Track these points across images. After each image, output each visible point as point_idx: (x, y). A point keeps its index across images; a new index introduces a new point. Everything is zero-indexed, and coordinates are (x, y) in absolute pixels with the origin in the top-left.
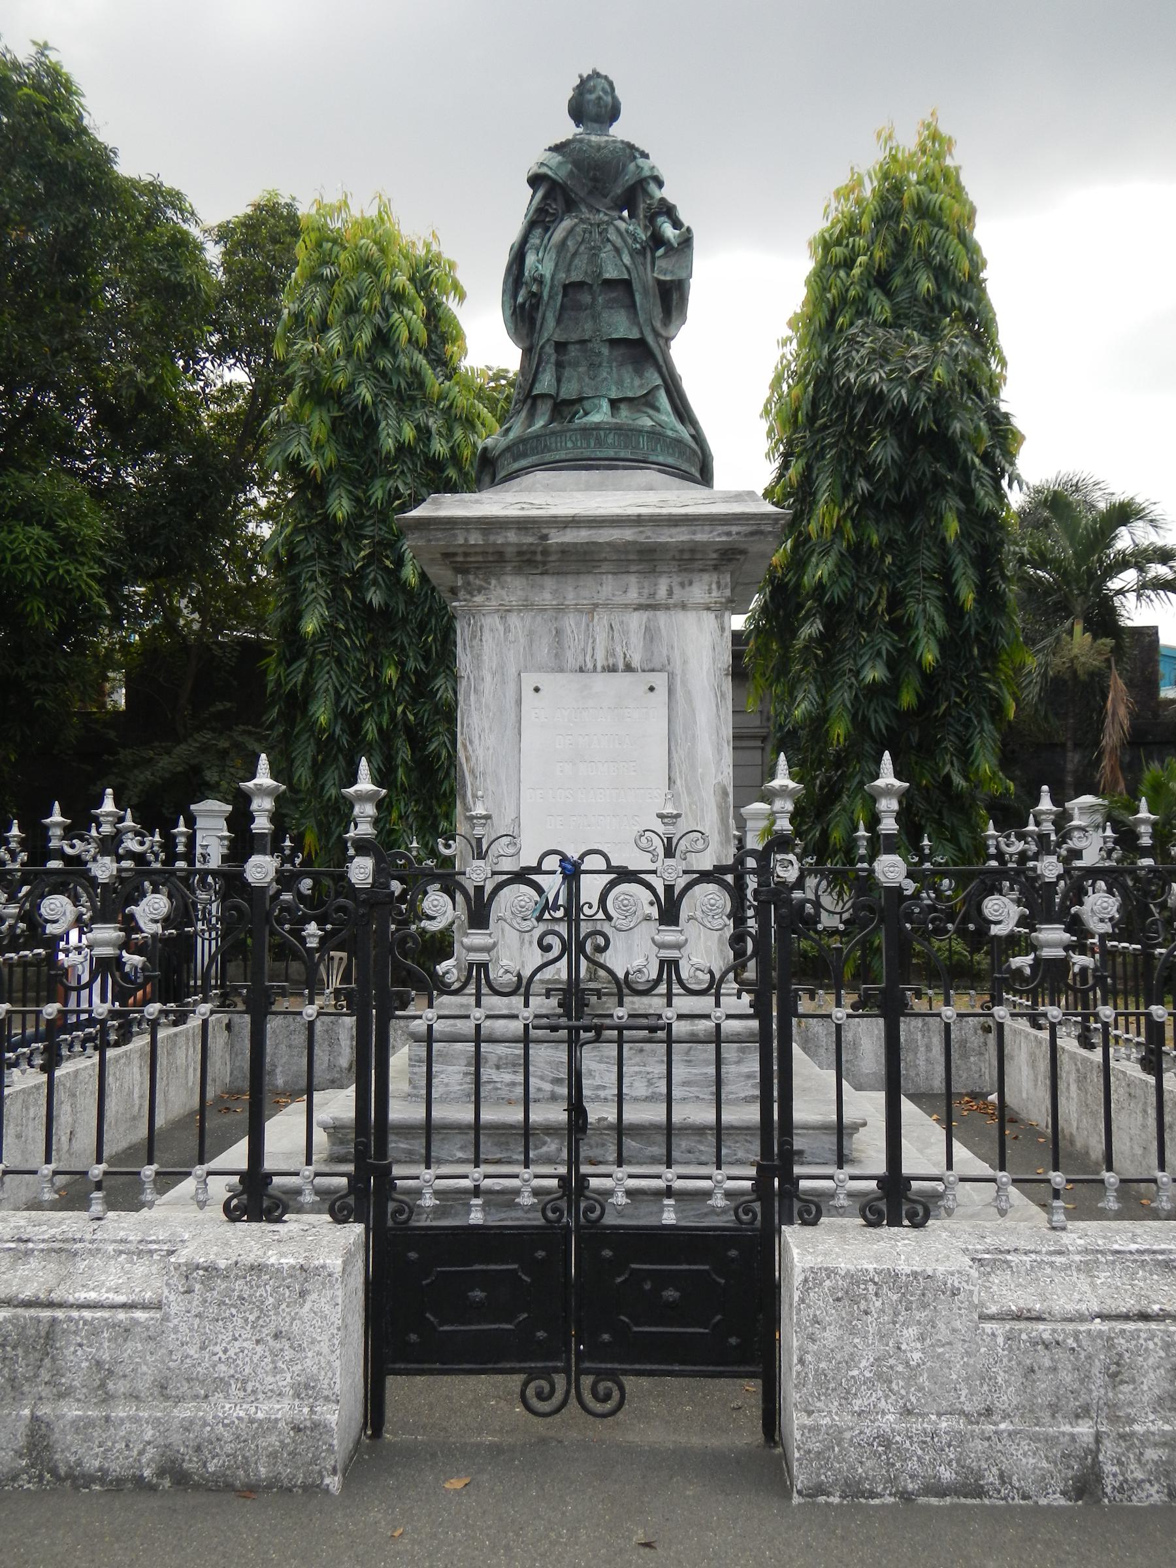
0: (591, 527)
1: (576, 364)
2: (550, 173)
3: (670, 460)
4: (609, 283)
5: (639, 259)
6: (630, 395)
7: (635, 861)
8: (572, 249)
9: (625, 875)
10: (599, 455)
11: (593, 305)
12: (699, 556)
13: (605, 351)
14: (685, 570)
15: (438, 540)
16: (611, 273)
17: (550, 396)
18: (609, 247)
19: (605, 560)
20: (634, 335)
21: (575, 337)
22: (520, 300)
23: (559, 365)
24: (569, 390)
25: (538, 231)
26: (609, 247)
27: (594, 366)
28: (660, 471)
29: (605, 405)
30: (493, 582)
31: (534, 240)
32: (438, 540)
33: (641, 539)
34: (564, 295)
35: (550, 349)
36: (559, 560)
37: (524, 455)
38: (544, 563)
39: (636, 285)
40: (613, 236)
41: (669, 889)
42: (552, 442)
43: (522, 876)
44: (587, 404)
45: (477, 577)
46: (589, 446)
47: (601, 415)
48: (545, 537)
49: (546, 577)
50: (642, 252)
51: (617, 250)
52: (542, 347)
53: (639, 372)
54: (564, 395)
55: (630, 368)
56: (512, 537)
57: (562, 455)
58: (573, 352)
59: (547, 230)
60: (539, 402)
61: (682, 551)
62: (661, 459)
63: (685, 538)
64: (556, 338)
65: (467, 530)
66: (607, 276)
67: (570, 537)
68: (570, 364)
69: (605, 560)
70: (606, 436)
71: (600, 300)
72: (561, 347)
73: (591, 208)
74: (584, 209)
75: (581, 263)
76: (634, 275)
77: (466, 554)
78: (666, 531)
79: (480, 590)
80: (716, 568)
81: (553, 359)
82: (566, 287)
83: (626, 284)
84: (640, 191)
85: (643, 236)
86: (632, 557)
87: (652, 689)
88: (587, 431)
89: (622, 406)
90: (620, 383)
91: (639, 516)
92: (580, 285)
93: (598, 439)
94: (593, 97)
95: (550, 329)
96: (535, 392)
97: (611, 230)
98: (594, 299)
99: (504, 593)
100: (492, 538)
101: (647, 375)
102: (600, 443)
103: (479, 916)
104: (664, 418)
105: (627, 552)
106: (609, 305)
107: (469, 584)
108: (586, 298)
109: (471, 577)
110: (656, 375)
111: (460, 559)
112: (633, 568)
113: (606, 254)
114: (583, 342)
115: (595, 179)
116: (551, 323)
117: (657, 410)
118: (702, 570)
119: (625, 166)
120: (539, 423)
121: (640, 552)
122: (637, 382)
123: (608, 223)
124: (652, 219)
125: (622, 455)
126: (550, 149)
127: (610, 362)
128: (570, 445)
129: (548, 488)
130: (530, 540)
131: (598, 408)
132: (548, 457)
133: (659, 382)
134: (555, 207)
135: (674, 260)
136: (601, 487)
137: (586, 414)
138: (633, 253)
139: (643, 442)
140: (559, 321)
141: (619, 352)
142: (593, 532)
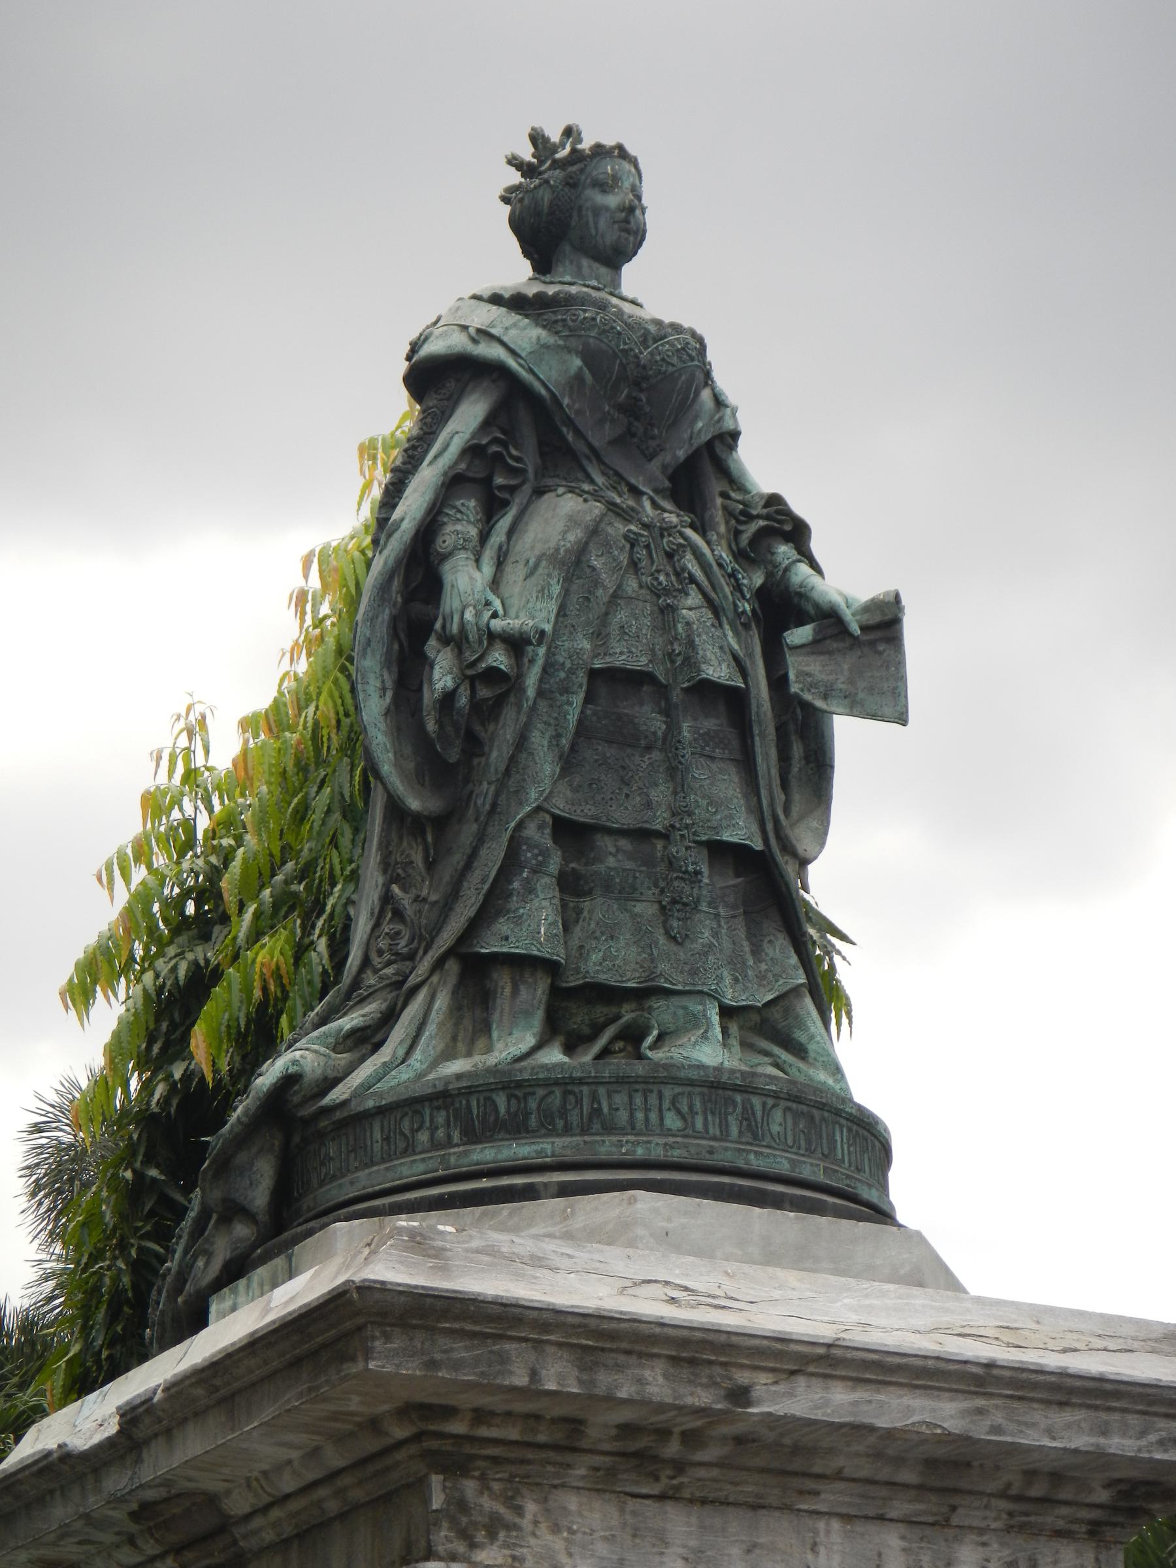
0: (859, 1381)
1: (627, 894)
2: (512, 363)
4: (706, 691)
10: (756, 1163)
12: (1065, 1494)
14: (1022, 1528)
15: (457, 1366)
17: (551, 967)
19: (838, 1476)
21: (623, 816)
23: (571, 886)
24: (613, 959)
27: (675, 908)
30: (531, 1508)
31: (461, 527)
32: (457, 1366)
33: (980, 1431)
34: (588, 700)
35: (539, 835)
36: (719, 1464)
37: (517, 1128)
38: (680, 1467)
44: (662, 1013)
45: (485, 1487)
46: (724, 1136)
48: (740, 1395)
49: (669, 1507)
52: (520, 825)
56: (655, 1383)
58: (613, 857)
60: (503, 981)
61: (1031, 1475)
63: (1081, 1441)
64: (561, 806)
65: (538, 1344)
67: (802, 1401)
68: (608, 888)
69: (838, 1476)
70: (767, 1112)
71: (686, 730)
77: (481, 1416)
78: (1041, 1417)
79: (494, 1527)
80: (1095, 1532)
81: (555, 863)
84: (708, 468)
86: (908, 1476)
91: (990, 1365)
92: (633, 680)
93: (747, 1116)
94: (612, 200)
96: (490, 945)
98: (672, 727)
99: (557, 1543)
100: (604, 1380)
105: (899, 1461)
107: (462, 1505)
109: (470, 1487)
111: (458, 1427)
112: (900, 1507)
114: (642, 835)
115: (631, 410)
116: (544, 764)
118: (1059, 1534)
121: (931, 1464)
126: (496, 299)
128: (672, 1121)
129: (669, 1242)
130: (703, 1398)
132: (607, 1147)
134: (527, 454)
135: (846, 663)
136: (801, 1259)
140: (568, 763)
142: (861, 1394)
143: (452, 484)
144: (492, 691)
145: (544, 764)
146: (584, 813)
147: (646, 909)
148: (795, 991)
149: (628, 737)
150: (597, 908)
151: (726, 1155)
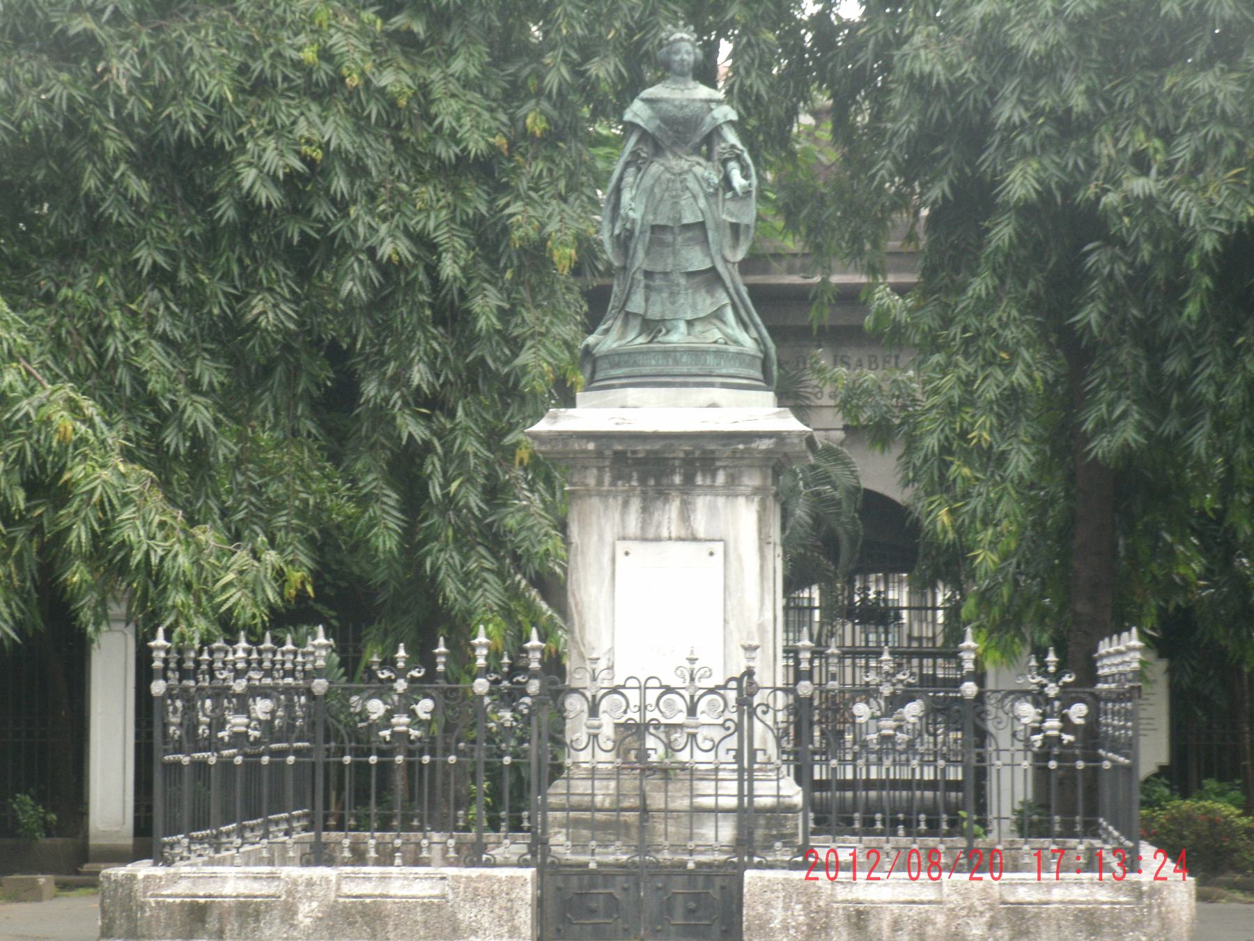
1: (659, 290)
3: (732, 371)
5: (712, 200)
6: (702, 315)
7: (675, 682)
8: (658, 196)
9: (669, 690)
11: (673, 244)
13: (683, 281)
16: (688, 219)
18: (688, 194)
20: (708, 265)
21: (659, 268)
22: (617, 232)
23: (647, 287)
24: (655, 312)
25: (632, 170)
26: (688, 194)
27: (673, 295)
29: (682, 326)
31: (629, 179)
35: (640, 276)
37: (618, 365)
39: (710, 224)
40: (692, 184)
41: (692, 697)
42: (640, 359)
43: (615, 690)
44: (669, 325)
47: (678, 337)
50: (715, 194)
51: (695, 197)
53: (710, 292)
54: (650, 316)
55: (703, 291)
57: (646, 370)
58: (658, 282)
59: (639, 169)
62: (724, 371)
64: (644, 267)
66: (685, 221)
71: (680, 239)
72: (648, 274)
73: (675, 154)
74: (670, 156)
75: (665, 209)
76: (709, 215)
82: (654, 228)
83: (702, 225)
84: (716, 139)
85: (716, 180)
87: (711, 554)
88: (669, 353)
90: (694, 307)
92: (663, 228)
95: (640, 260)
97: (690, 177)
102: (677, 362)
103: (594, 711)
104: (729, 331)
106: (687, 242)
108: (669, 238)
110: (724, 295)
113: (686, 200)
114: (666, 274)
115: (677, 132)
116: (640, 254)
117: (724, 322)
120: (632, 335)
122: (709, 301)
123: (690, 171)
124: (724, 163)
125: (694, 370)
131: (676, 328)
132: (636, 370)
133: (727, 301)
137: (668, 332)
139: (710, 360)
140: (647, 253)
143: (627, 165)
144: (630, 234)
145: (640, 254)
146: (650, 269)
147: (665, 295)
149: (662, 244)
150: (654, 297)
151: (667, 370)
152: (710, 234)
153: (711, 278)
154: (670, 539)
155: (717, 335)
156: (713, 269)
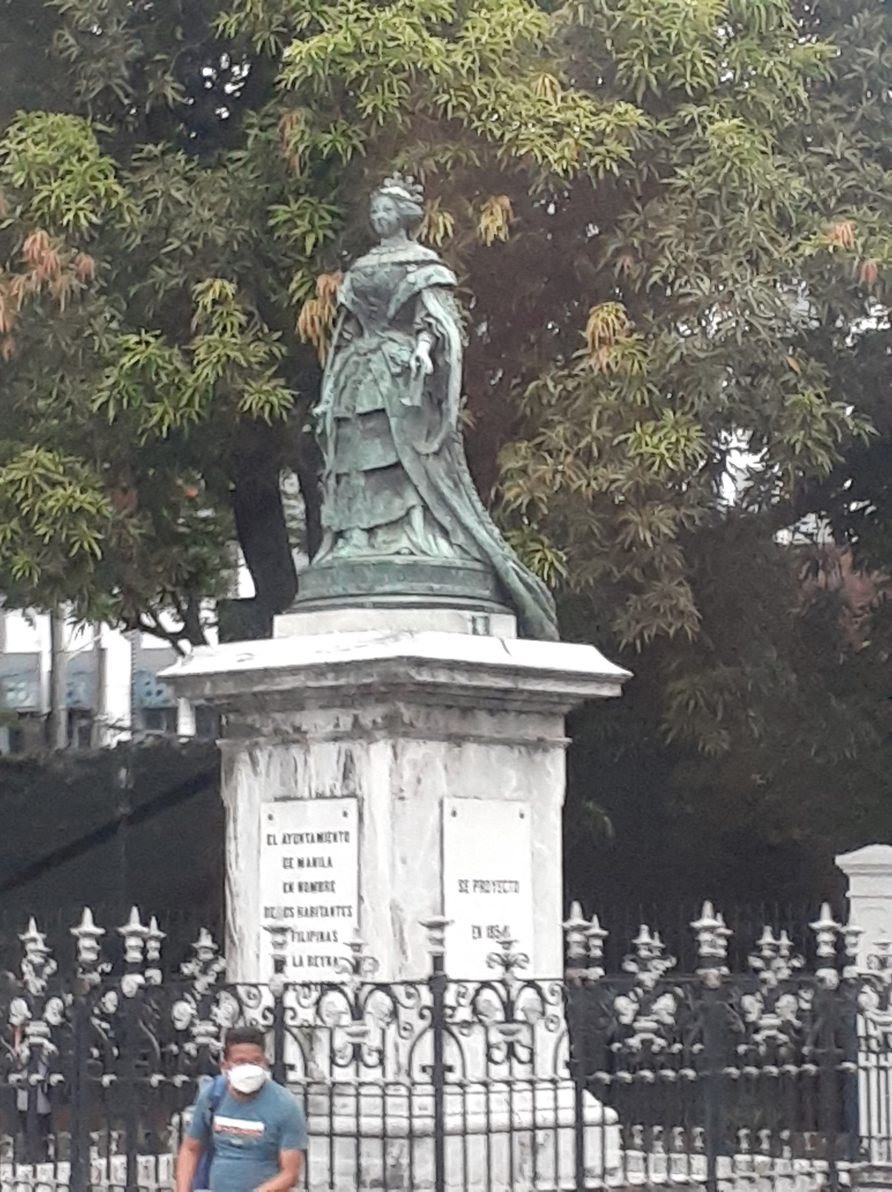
8: (342, 384)
13: (362, 481)
16: (364, 406)
20: (391, 460)
28: (376, 606)
47: (354, 549)
53: (399, 494)
66: (360, 410)
89: (380, 532)
90: (370, 512)
101: (406, 494)
119: (396, 285)
127: (364, 490)
138: (394, 376)
141: (373, 480)
148: (413, 507)
152: (393, 422)
153: (392, 475)
154: (311, 798)
155: (404, 543)
156: (398, 465)
